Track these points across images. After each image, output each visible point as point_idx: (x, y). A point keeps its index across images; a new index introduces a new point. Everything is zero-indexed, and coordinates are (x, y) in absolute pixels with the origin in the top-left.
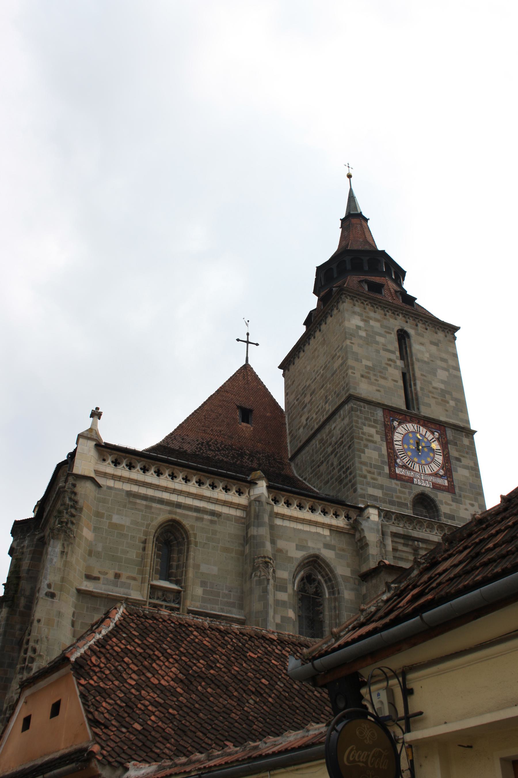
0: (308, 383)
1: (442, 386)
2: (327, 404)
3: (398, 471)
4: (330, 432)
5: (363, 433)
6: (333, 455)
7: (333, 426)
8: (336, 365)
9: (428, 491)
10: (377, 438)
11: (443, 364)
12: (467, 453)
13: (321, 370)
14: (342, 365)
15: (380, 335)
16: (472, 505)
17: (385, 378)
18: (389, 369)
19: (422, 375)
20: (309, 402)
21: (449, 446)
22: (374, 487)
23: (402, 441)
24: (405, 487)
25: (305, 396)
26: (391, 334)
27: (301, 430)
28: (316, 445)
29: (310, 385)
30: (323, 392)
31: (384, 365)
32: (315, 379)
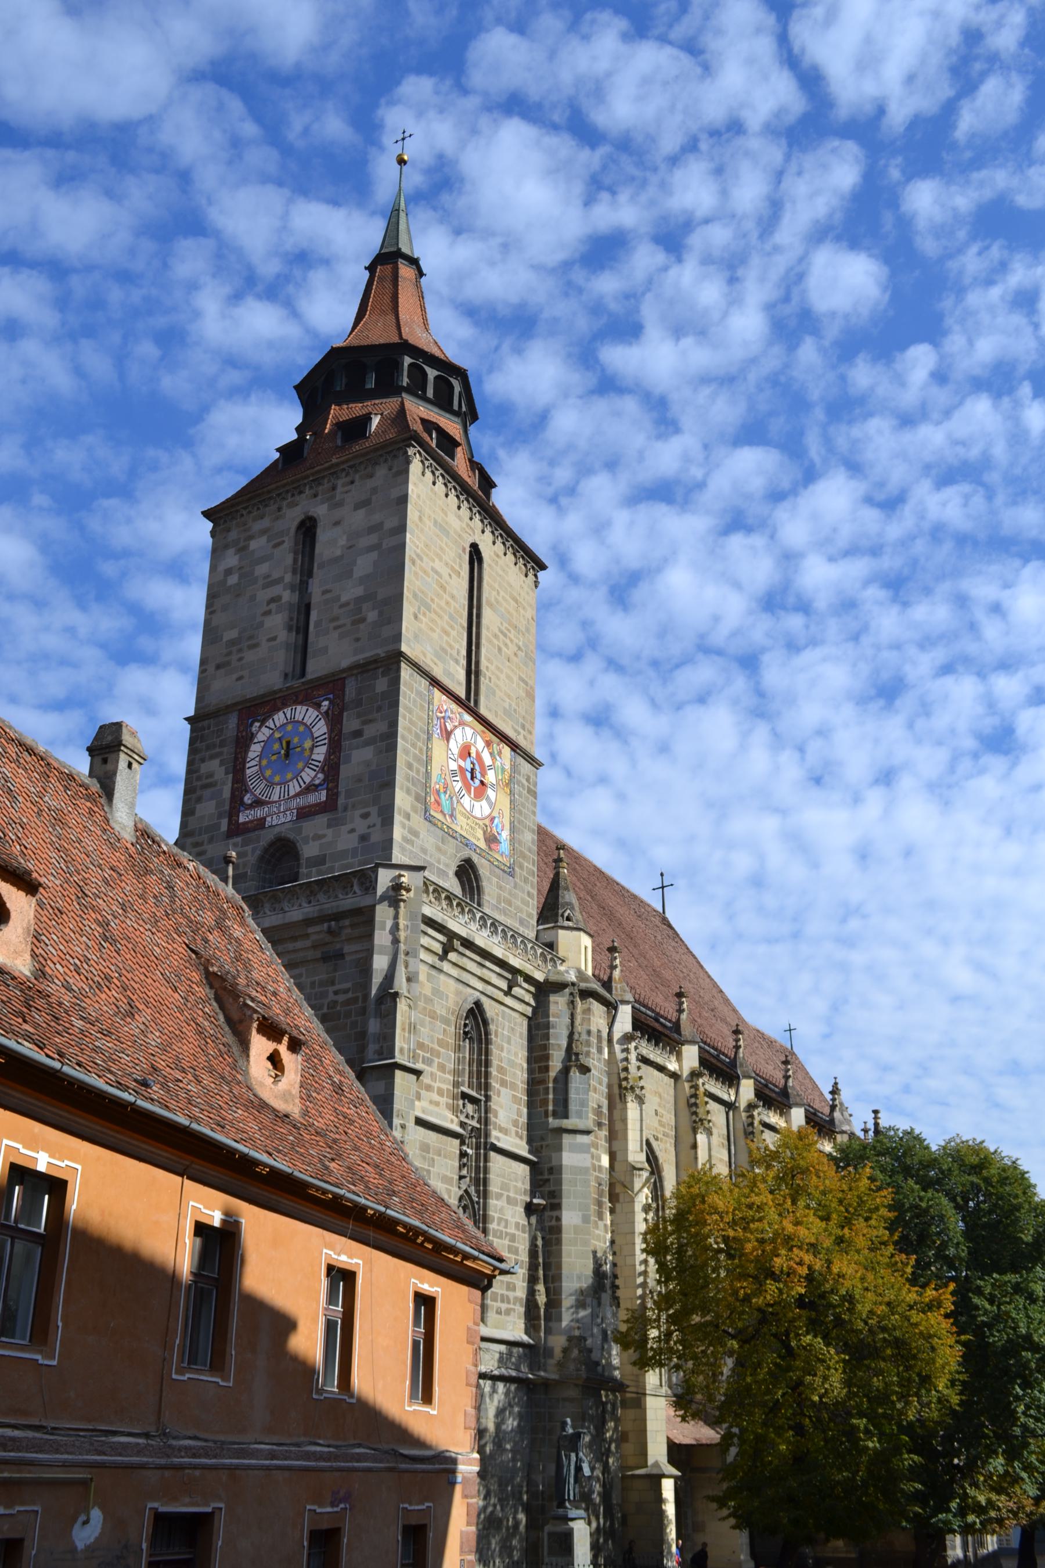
3: (242, 819)
16: (366, 816)
21: (345, 714)
23: (261, 756)
26: (283, 542)
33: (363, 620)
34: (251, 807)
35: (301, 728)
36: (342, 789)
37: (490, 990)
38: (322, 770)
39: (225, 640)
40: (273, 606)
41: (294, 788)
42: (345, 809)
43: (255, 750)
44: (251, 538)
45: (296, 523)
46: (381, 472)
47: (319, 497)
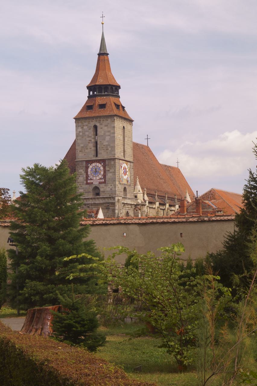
1: (107, 143)
3: (89, 181)
5: (79, 172)
9: (97, 185)
10: (83, 172)
11: (107, 134)
12: (112, 167)
15: (87, 131)
16: (111, 185)
17: (86, 149)
18: (89, 144)
19: (100, 142)
22: (81, 189)
24: (90, 186)
31: (87, 144)
33: (108, 149)
34: (90, 180)
35: (98, 167)
36: (107, 180)
37: (129, 208)
38: (103, 176)
39: (81, 146)
40: (90, 142)
41: (98, 178)
42: (108, 184)
43: (89, 170)
44: (84, 126)
45: (93, 125)
46: (109, 120)
47: (97, 122)
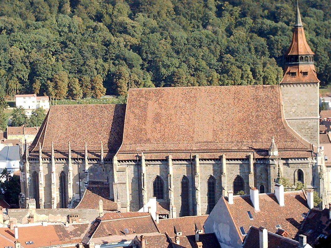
0: (296, 100)
2: (306, 113)
4: (307, 122)
6: (308, 130)
7: (309, 122)
8: (312, 104)
13: (304, 100)
14: (315, 106)
20: (297, 106)
25: (294, 103)
27: (291, 113)
28: (300, 122)
29: (297, 101)
30: (304, 108)
32: (300, 101)
